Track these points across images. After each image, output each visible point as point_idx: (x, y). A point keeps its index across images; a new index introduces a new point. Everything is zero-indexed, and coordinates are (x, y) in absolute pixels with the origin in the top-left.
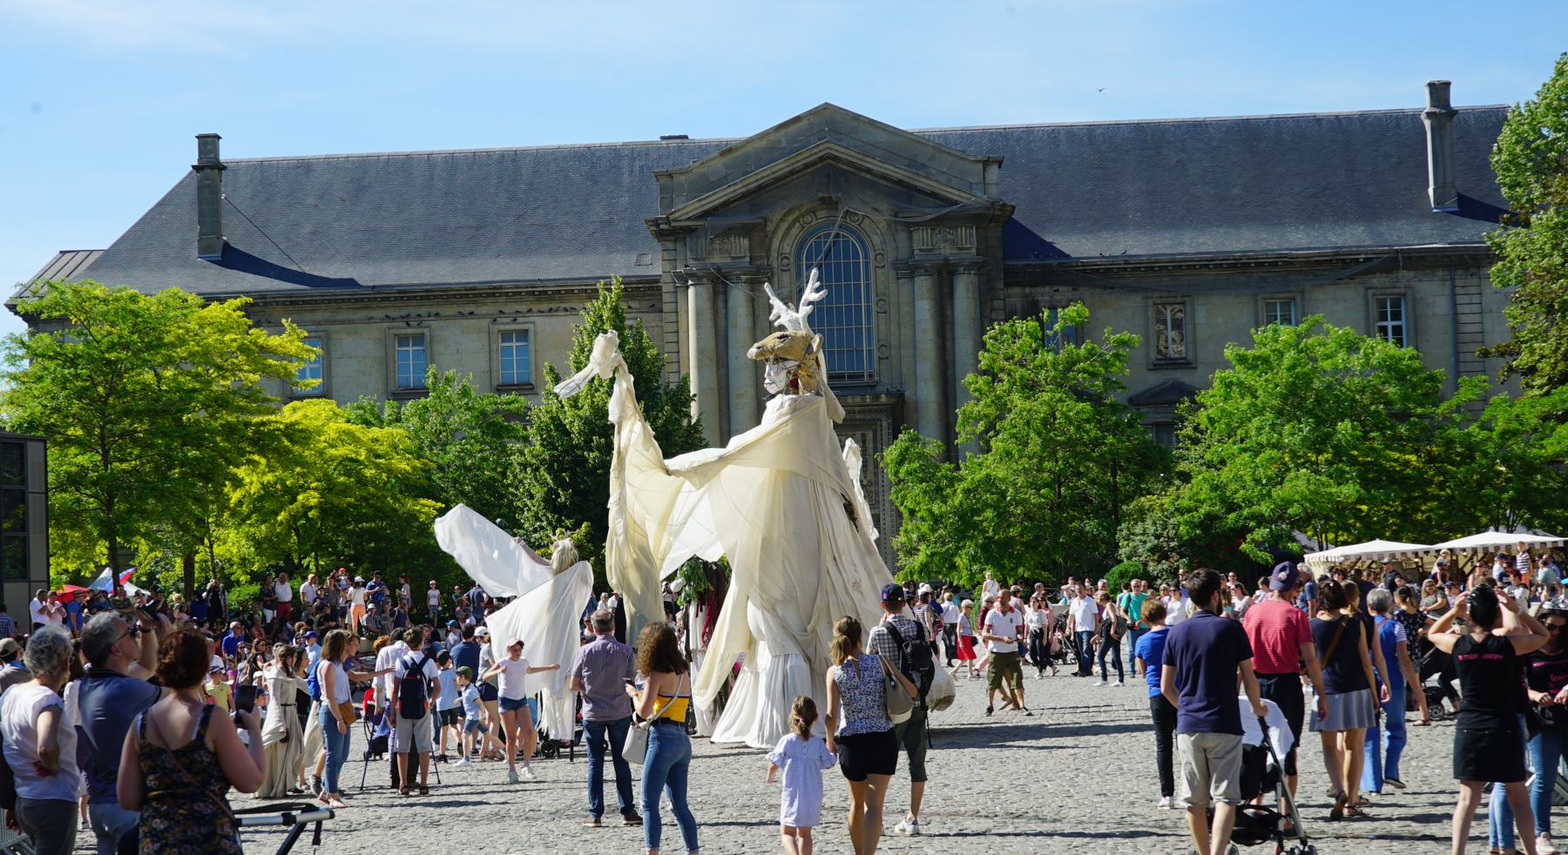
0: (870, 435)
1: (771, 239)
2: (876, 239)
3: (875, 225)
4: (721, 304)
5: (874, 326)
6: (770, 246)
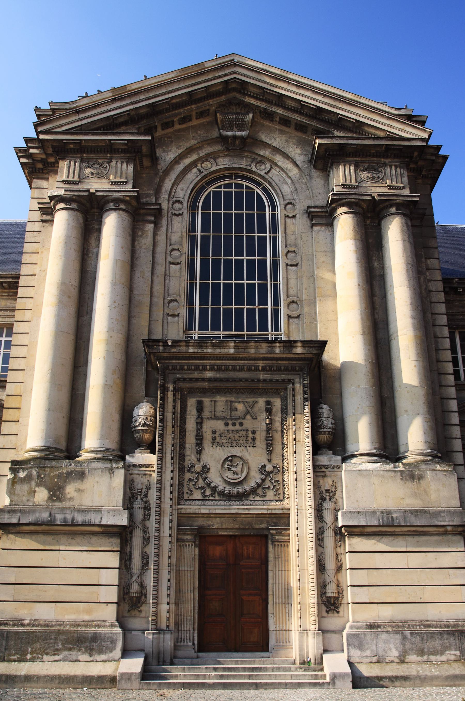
0: (277, 403)
1: (162, 181)
2: (286, 189)
3: (286, 172)
5: (281, 283)
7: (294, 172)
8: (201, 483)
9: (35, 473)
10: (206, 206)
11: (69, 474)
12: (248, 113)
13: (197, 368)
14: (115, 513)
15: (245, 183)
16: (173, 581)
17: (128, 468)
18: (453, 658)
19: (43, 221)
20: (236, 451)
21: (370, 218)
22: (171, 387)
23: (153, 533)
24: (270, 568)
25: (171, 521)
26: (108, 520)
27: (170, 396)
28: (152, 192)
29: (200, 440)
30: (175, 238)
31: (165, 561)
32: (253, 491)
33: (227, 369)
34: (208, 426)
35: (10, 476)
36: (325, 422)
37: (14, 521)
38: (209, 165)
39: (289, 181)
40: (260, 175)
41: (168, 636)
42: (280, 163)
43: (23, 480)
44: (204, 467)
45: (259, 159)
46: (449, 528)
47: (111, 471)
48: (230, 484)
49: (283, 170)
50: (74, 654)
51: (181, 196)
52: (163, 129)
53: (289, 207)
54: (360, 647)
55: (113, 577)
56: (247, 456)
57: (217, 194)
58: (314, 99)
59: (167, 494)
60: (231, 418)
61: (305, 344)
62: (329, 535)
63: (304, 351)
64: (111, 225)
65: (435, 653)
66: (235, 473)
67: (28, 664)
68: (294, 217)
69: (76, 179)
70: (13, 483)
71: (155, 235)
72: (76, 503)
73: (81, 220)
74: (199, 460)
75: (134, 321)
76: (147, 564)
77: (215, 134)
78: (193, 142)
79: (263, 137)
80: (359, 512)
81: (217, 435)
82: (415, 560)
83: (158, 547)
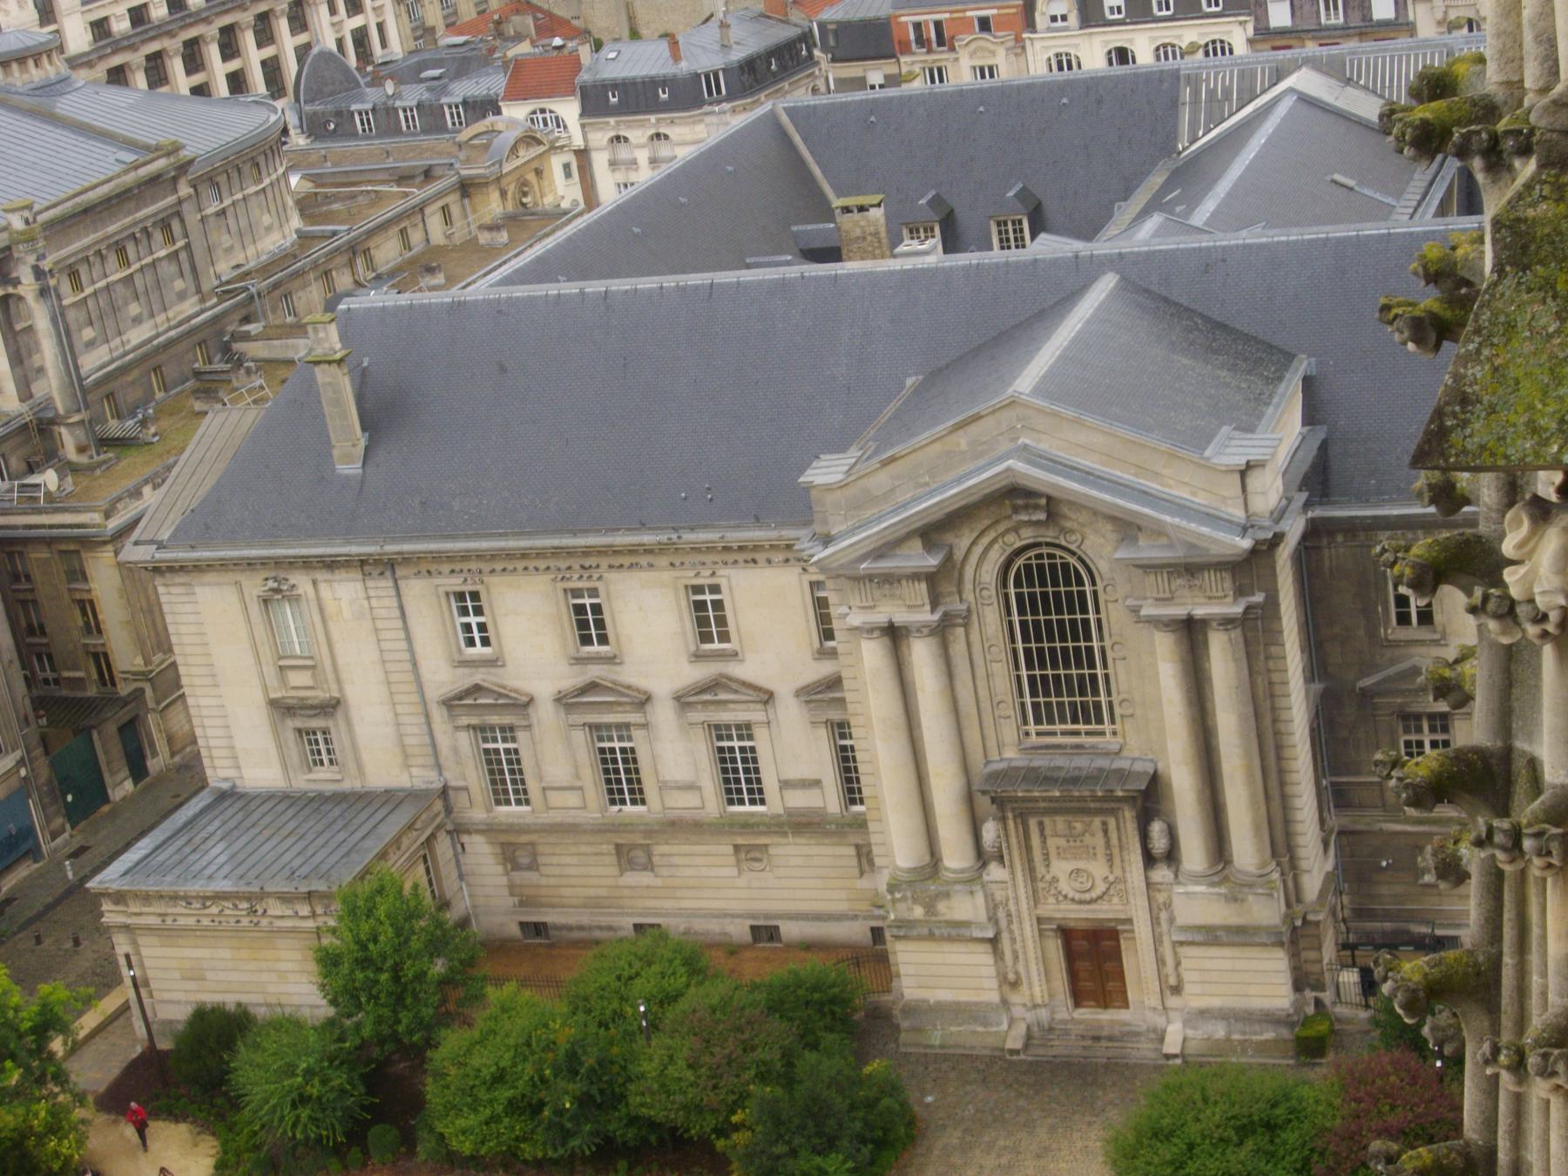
6: (961, 576)
9: (909, 894)
10: (1018, 584)
15: (1058, 553)
20: (1081, 865)
22: (1010, 815)
23: (1017, 933)
26: (977, 934)
27: (1011, 823)
28: (954, 589)
31: (1031, 955)
32: (1100, 897)
34: (1052, 842)
47: (972, 893)
54: (1195, 1028)
55: (992, 971)
57: (1028, 567)
60: (1070, 836)
64: (921, 654)
65: (1255, 1033)
72: (948, 917)
78: (987, 522)
82: (1240, 965)
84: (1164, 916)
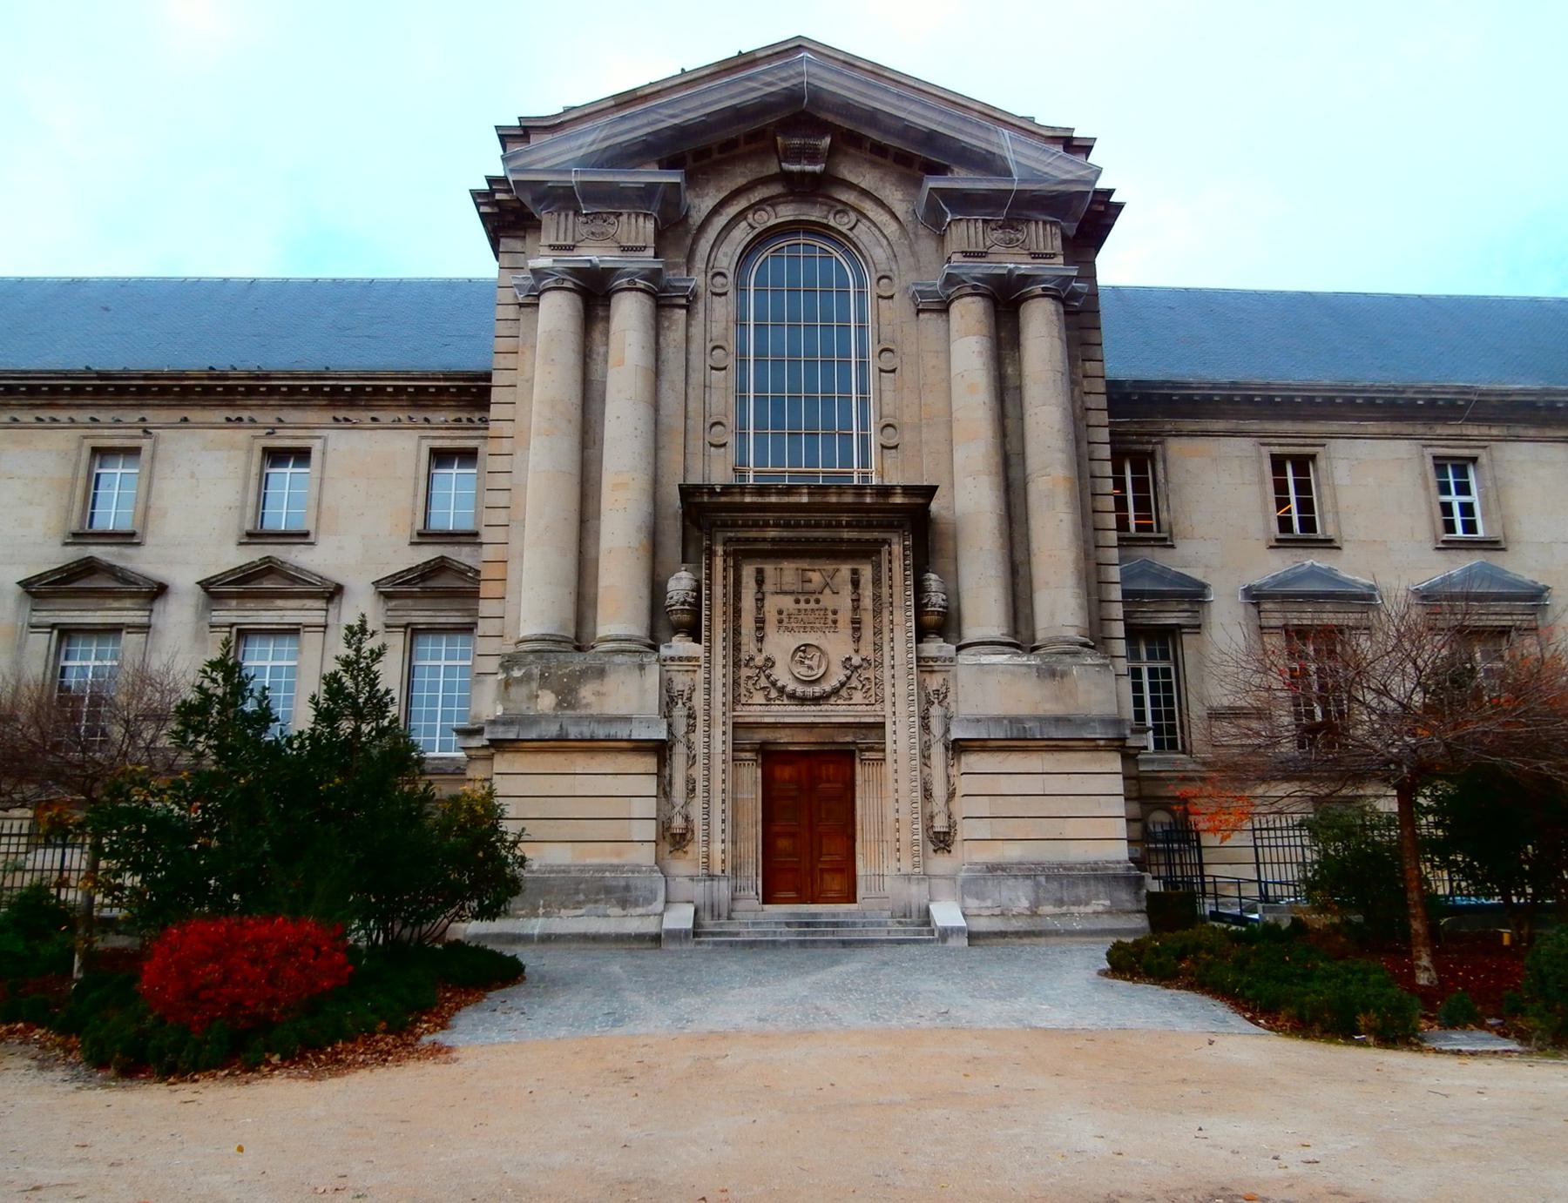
0: (867, 571)
1: (695, 241)
2: (879, 254)
4: (597, 336)
7: (891, 228)
8: (763, 682)
9: (536, 671)
11: (583, 673)
12: (822, 136)
13: (756, 525)
14: (648, 722)
16: (729, 813)
17: (663, 662)
18: (1100, 908)
19: (521, 305)
20: (811, 638)
21: (1005, 301)
22: (720, 550)
23: (700, 750)
24: (858, 794)
25: (724, 733)
26: (641, 733)
27: (719, 562)
28: (682, 260)
29: (760, 623)
30: (717, 329)
31: (717, 786)
32: (835, 692)
33: (797, 525)
34: (772, 604)
35: (501, 676)
36: (934, 600)
37: (512, 736)
38: (765, 217)
39: (885, 242)
40: (840, 233)
41: (724, 884)
42: (870, 214)
43: (519, 681)
44: (768, 659)
45: (840, 207)
46: (1102, 743)
47: (642, 667)
48: (804, 682)
49: (875, 225)
50: (601, 907)
51: (725, 264)
52: (695, 161)
53: (884, 281)
54: (979, 896)
55: (649, 807)
56: (824, 645)
58: (924, 117)
59: (718, 698)
60: (803, 594)
61: (908, 490)
62: (938, 752)
63: (906, 501)
65: (1078, 903)
66: (810, 667)
67: (541, 920)
68: (891, 297)
69: (569, 242)
70: (507, 684)
71: (688, 325)
72: (594, 711)
73: (579, 304)
74: (760, 651)
75: (663, 454)
76: (694, 790)
77: (772, 168)
78: (741, 181)
79: (847, 172)
80: (978, 721)
81: (784, 617)
83: (708, 768)
84: (936, 711)
